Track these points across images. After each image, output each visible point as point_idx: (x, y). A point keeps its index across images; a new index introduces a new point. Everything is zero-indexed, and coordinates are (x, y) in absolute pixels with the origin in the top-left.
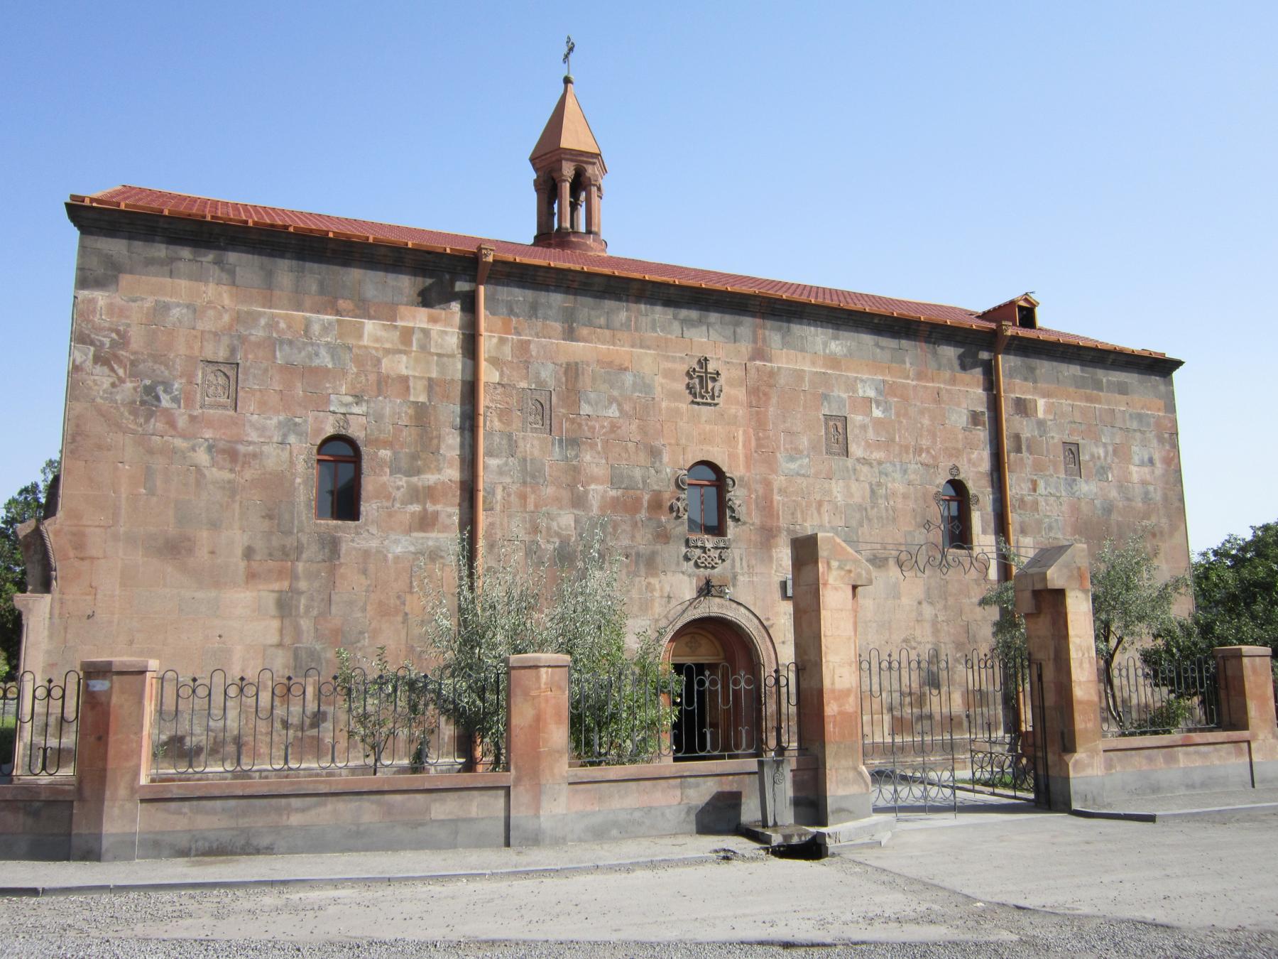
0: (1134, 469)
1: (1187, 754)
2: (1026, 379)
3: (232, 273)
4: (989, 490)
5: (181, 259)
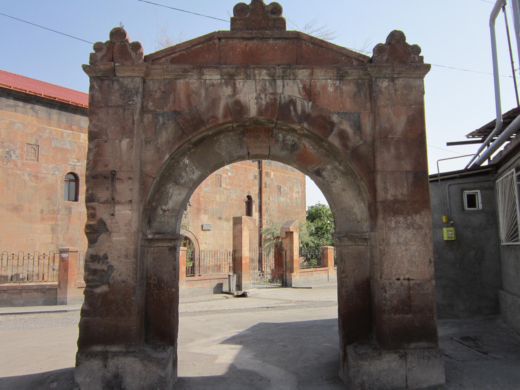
0: (294, 194)
1: (315, 273)
2: (269, 166)
3: (37, 113)
4: (258, 199)
5: (19, 106)
